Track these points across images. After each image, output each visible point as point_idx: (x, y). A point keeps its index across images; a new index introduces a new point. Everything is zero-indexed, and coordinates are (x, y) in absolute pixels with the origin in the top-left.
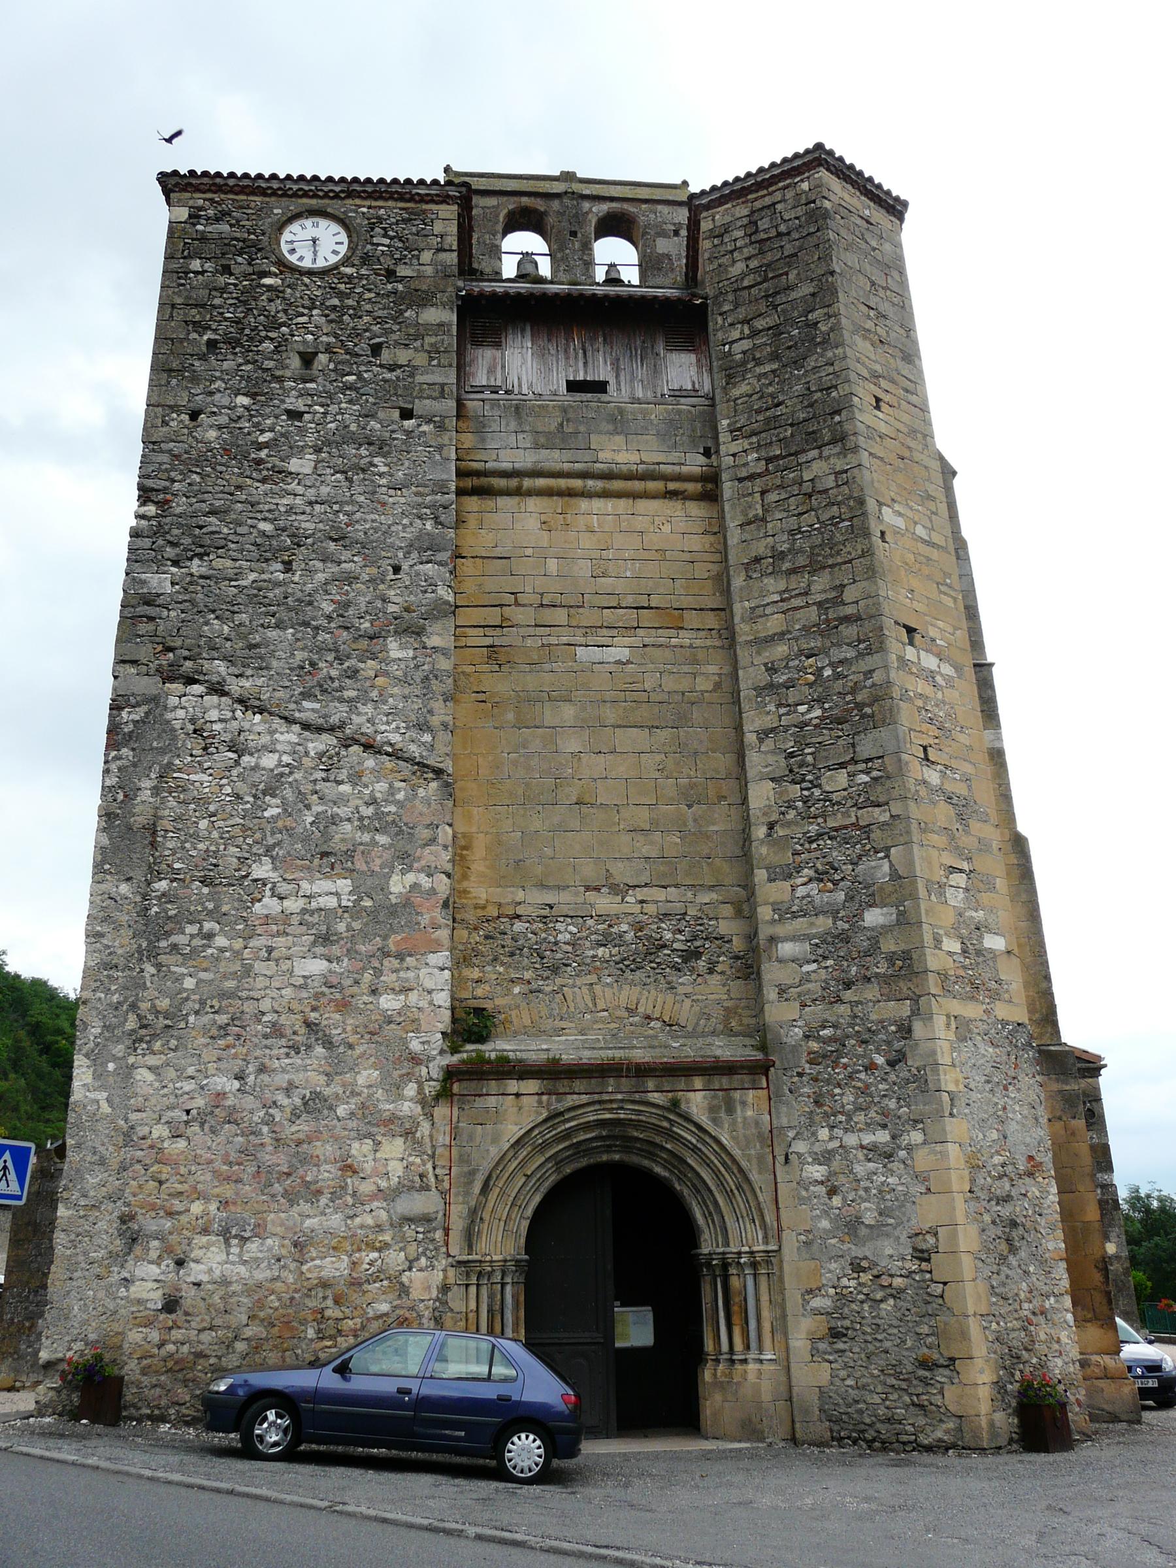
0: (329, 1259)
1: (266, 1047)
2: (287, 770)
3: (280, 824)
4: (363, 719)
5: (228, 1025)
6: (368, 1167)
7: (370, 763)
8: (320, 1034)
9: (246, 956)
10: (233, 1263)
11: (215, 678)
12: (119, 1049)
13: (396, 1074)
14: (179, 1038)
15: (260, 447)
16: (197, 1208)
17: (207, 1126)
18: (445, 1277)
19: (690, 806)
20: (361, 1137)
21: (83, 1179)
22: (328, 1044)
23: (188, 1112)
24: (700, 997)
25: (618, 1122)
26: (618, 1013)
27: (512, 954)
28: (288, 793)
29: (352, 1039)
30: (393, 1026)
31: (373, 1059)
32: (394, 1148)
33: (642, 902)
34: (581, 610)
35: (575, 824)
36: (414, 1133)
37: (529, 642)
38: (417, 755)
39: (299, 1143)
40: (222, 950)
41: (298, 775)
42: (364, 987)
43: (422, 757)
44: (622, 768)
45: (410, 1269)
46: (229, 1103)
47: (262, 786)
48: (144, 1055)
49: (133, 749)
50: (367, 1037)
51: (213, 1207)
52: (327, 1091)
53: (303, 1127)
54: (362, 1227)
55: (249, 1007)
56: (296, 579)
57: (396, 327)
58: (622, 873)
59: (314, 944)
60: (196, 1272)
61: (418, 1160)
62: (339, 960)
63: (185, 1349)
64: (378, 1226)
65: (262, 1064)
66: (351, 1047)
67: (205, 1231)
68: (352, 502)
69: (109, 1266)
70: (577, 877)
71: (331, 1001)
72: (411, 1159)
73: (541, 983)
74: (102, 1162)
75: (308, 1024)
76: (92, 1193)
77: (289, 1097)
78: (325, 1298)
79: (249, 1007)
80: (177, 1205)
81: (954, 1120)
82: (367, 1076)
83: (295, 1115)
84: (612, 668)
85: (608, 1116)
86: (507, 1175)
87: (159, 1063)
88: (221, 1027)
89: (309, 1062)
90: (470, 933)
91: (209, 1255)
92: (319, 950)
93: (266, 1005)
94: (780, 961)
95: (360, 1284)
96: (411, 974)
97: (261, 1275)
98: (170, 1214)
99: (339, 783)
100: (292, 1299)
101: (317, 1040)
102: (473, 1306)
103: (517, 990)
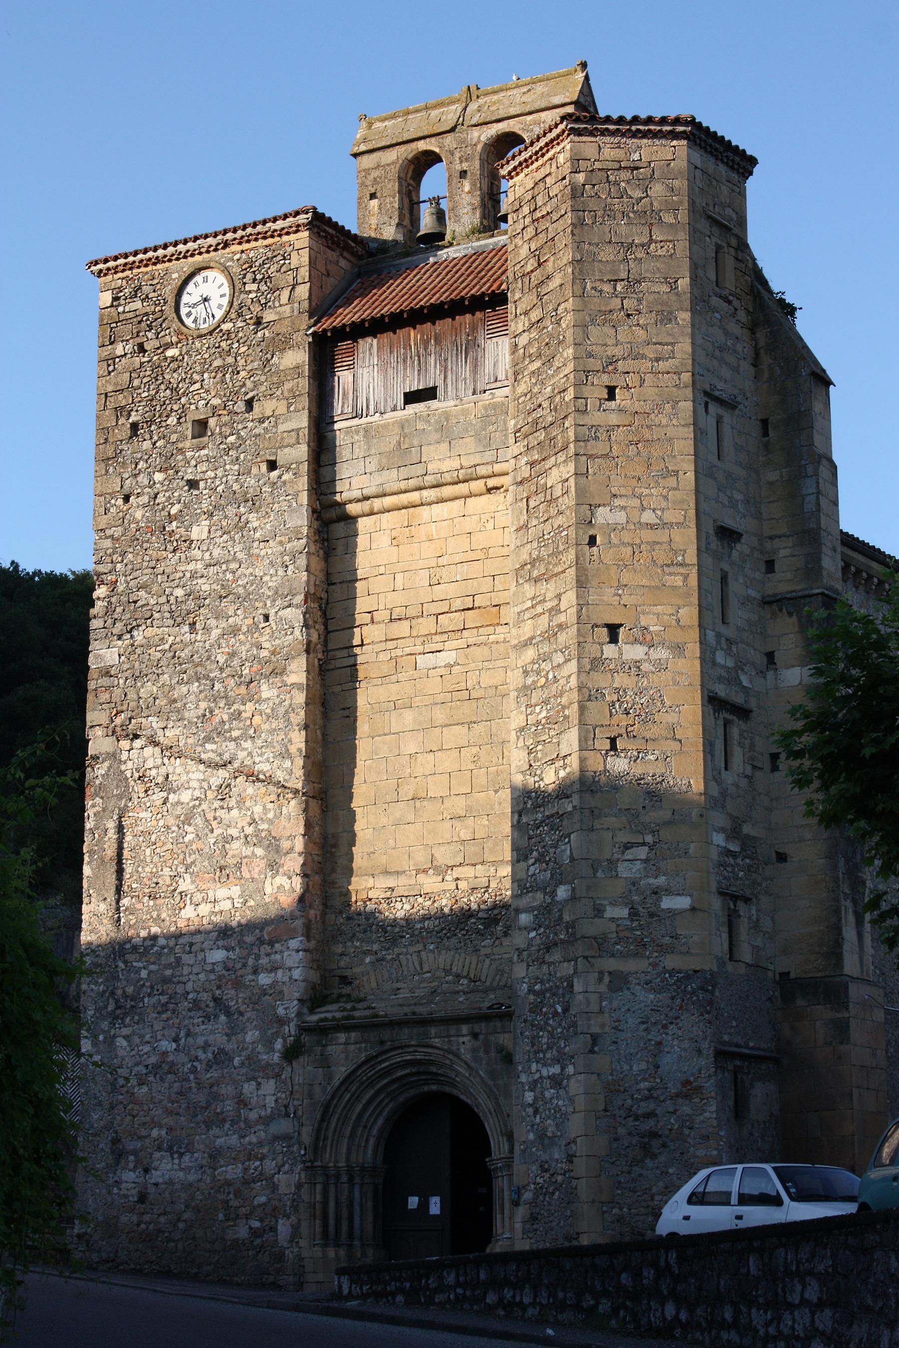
0: (231, 1167)
1: (191, 1017)
2: (197, 802)
3: (194, 847)
4: (245, 753)
5: (167, 1003)
6: (254, 1101)
7: (250, 790)
8: (222, 1006)
9: (177, 951)
10: (176, 1170)
11: (149, 732)
12: (105, 1025)
13: (270, 1032)
14: (140, 1014)
15: (170, 518)
16: (155, 1133)
17: (158, 1076)
18: (300, 1178)
19: (496, 792)
20: (249, 1080)
21: (90, 1116)
22: (228, 1014)
23: (147, 1066)
24: (497, 957)
25: (418, 1062)
26: (438, 974)
27: (365, 931)
28: (199, 821)
29: (243, 1008)
30: (267, 997)
31: (255, 1023)
32: (269, 1086)
33: (458, 879)
34: (420, 620)
35: (411, 817)
36: (280, 1076)
37: (382, 657)
38: (281, 779)
39: (211, 1086)
40: (163, 948)
41: (204, 806)
42: (249, 969)
43: (285, 780)
44: (447, 762)
45: (279, 1172)
46: (170, 1058)
47: (182, 818)
48: (120, 1028)
49: (102, 798)
50: (251, 1006)
51: (163, 1132)
52: (229, 1047)
53: (214, 1074)
54: (250, 1143)
55: (180, 989)
56: (199, 638)
57: (263, 378)
58: (444, 856)
59: (217, 940)
60: (156, 1176)
61: (283, 1096)
62: (233, 949)
63: (151, 1227)
64: (260, 1143)
65: (189, 1030)
66: (241, 1014)
67: (159, 1149)
68: (234, 559)
69: (107, 1173)
70: (411, 862)
71: (230, 980)
72: (279, 1095)
73: (384, 953)
74: (100, 1104)
75: (215, 999)
76: (96, 1125)
77: (205, 1053)
78: (229, 1193)
79: (180, 989)
80: (144, 1132)
81: (595, 1056)
82: (251, 1035)
83: (209, 1067)
84: (442, 671)
85: (409, 1057)
86: (343, 1104)
87: (129, 1033)
88: (163, 1005)
89: (216, 1026)
90: (336, 917)
91: (163, 1165)
92: (220, 943)
93: (190, 986)
94: (520, 929)
95: (249, 1183)
96: (278, 957)
97: (192, 1177)
98: (140, 1138)
99: (229, 809)
100: (210, 1193)
101: (220, 1010)
102: (318, 1197)
103: (368, 960)
